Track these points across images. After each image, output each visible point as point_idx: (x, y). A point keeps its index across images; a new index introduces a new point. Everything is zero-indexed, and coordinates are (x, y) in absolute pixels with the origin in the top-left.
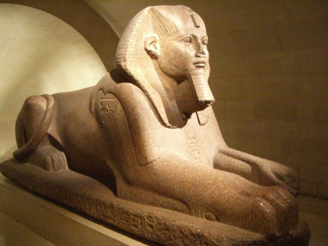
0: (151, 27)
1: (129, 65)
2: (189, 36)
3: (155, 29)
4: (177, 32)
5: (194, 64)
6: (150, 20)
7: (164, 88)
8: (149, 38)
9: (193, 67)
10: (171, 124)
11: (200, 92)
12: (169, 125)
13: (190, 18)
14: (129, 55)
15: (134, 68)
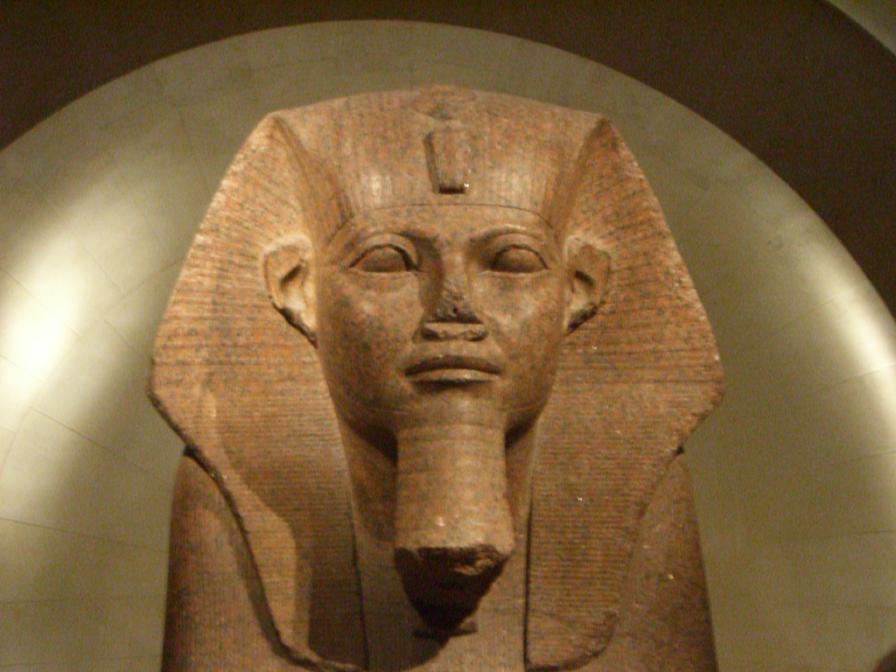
0: (294, 202)
1: (169, 382)
2: (388, 238)
3: (304, 209)
4: (344, 223)
5: (411, 371)
6: (286, 174)
7: (353, 478)
8: (274, 254)
9: (405, 385)
10: (319, 654)
11: (413, 508)
12: (307, 653)
13: (421, 153)
14: (169, 338)
15: (197, 390)
